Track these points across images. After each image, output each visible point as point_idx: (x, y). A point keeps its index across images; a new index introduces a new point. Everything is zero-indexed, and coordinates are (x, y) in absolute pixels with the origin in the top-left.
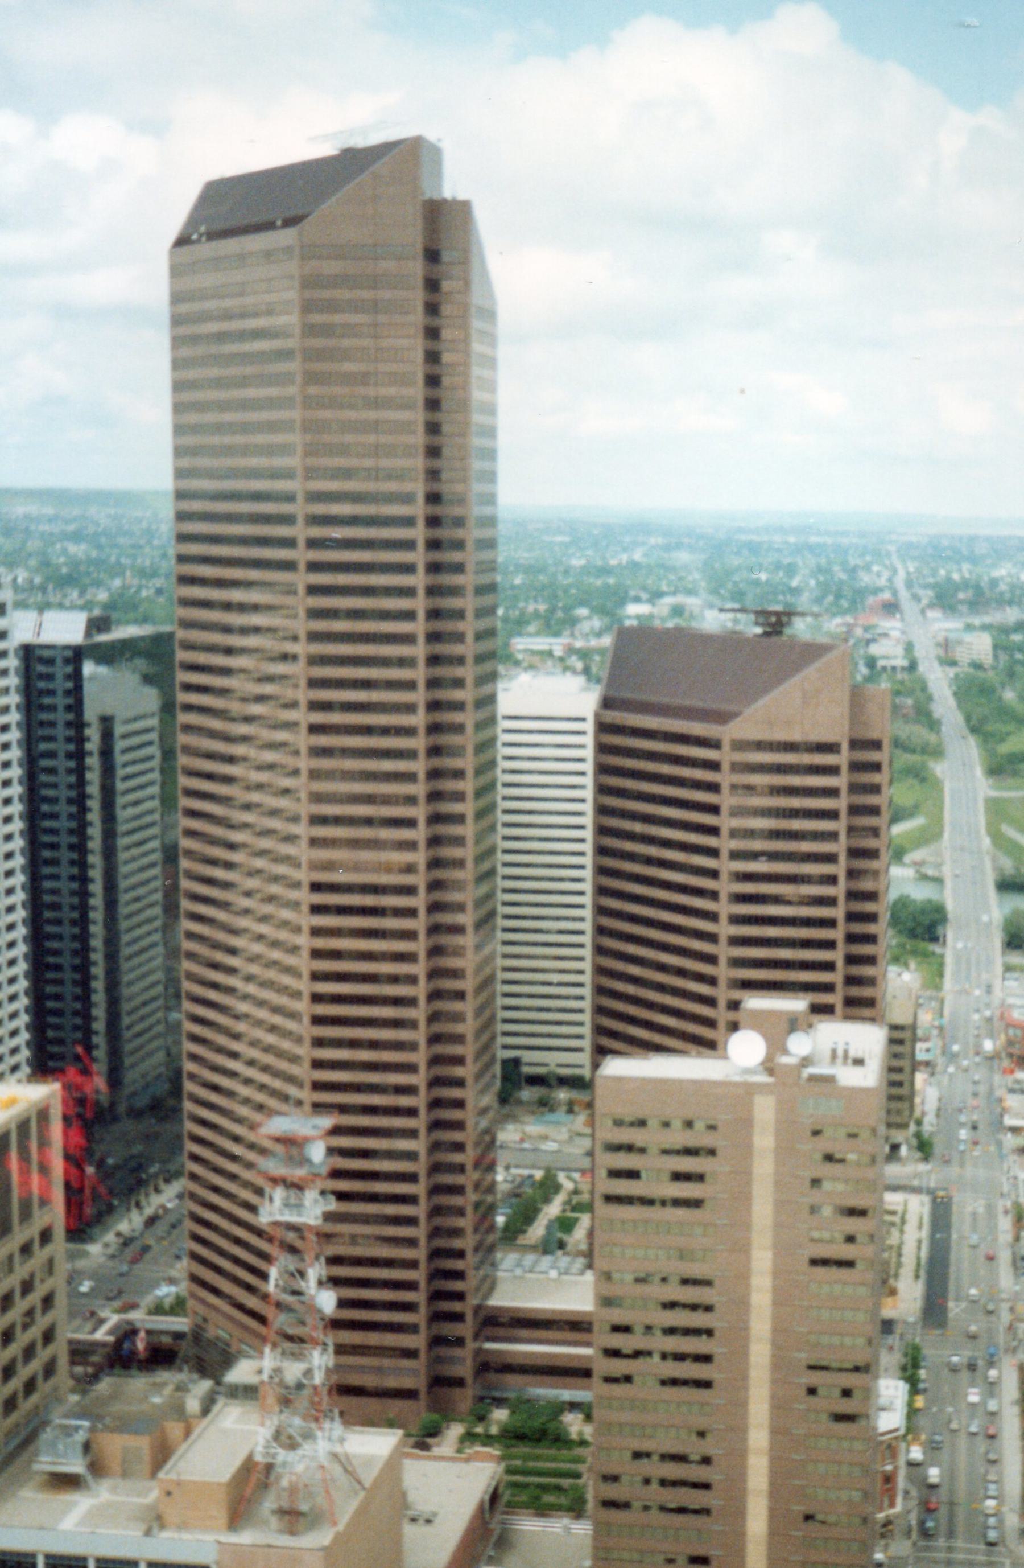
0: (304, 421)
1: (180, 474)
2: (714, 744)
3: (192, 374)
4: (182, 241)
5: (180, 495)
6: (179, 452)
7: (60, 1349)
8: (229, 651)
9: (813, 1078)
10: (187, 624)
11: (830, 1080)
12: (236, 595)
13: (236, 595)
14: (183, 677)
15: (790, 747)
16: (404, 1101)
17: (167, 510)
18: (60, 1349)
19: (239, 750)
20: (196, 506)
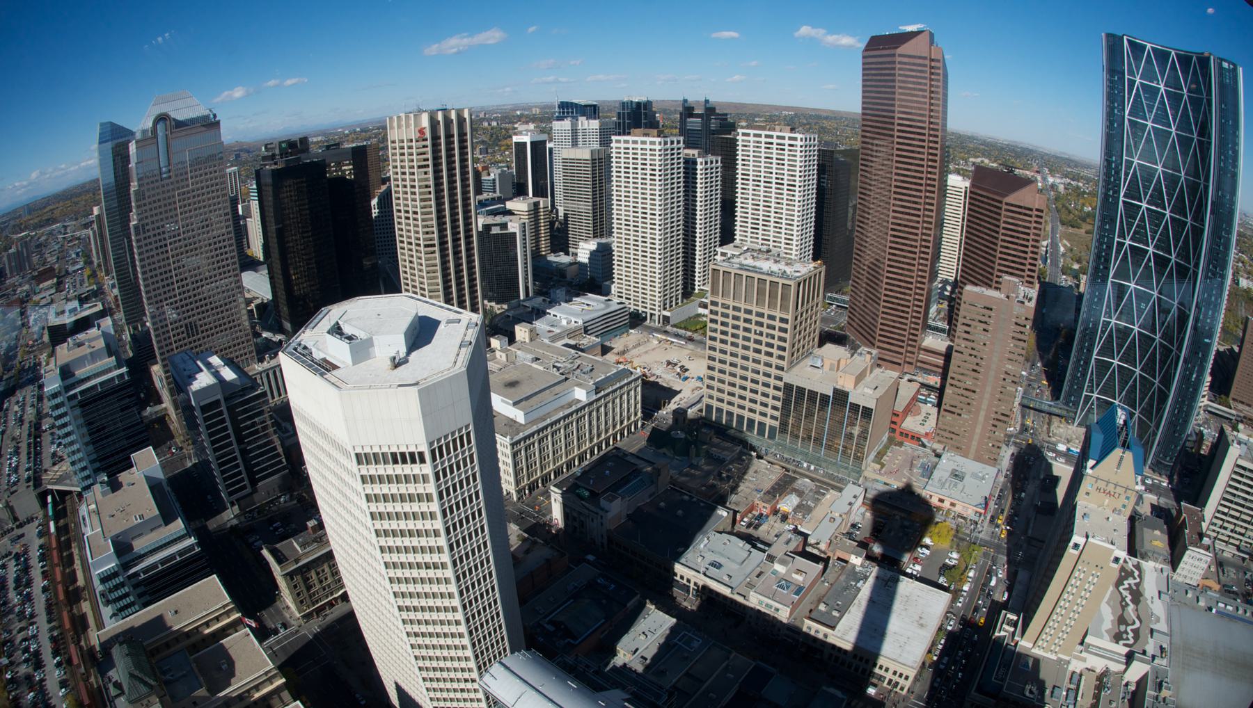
1: (863, 108)
2: (1001, 202)
3: (868, 83)
5: (863, 114)
6: (863, 103)
8: (872, 156)
10: (863, 148)
11: (1023, 303)
12: (876, 142)
13: (876, 142)
14: (861, 162)
15: (1020, 207)
16: (909, 286)
17: (860, 118)
19: (873, 183)
20: (868, 117)
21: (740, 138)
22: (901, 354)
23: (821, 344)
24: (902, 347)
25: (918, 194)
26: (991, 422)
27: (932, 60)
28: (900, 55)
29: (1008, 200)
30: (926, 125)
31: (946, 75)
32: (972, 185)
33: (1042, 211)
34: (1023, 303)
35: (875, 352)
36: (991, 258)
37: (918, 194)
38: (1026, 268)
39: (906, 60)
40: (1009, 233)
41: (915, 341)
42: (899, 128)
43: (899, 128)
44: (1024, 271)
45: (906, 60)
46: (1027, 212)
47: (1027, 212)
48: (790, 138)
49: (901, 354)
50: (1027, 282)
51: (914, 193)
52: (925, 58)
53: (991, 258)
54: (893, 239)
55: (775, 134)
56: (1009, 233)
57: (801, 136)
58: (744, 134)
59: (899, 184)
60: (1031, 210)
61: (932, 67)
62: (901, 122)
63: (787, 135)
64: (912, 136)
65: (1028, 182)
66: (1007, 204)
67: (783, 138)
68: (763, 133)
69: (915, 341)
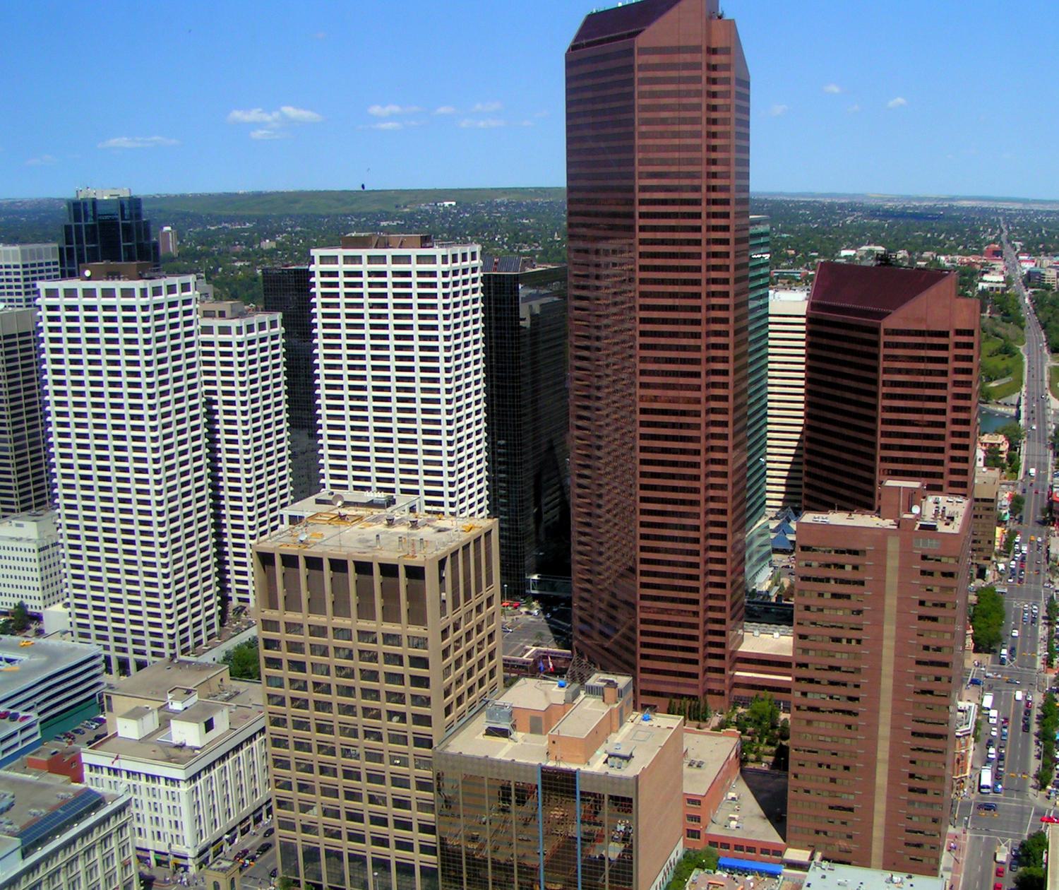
0: (729, 152)
4: (573, 48)
7: (498, 660)
9: (923, 527)
11: (933, 528)
13: (602, 246)
17: (563, 199)
18: (498, 660)
21: (316, 267)
22: (695, 676)
23: (509, 683)
24: (695, 662)
25: (692, 342)
26: (907, 783)
27: (713, 51)
28: (644, 51)
29: (886, 324)
30: (703, 195)
31: (745, 84)
32: (812, 306)
33: (970, 333)
34: (933, 528)
35: (623, 681)
36: (863, 449)
37: (692, 342)
38: (944, 457)
39: (655, 59)
40: (899, 391)
41: (722, 645)
42: (644, 209)
43: (644, 209)
44: (940, 463)
45: (655, 59)
46: (936, 340)
47: (936, 340)
48: (420, 259)
49: (695, 676)
50: (952, 484)
51: (684, 342)
52: (696, 49)
53: (863, 449)
54: (646, 443)
55: (389, 253)
56: (899, 391)
57: (443, 251)
58: (324, 260)
59: (648, 327)
60: (944, 334)
61: (713, 68)
62: (647, 196)
63: (414, 252)
64: (672, 222)
65: (934, 275)
66: (887, 332)
67: (407, 259)
68: (364, 253)
69: (722, 645)
